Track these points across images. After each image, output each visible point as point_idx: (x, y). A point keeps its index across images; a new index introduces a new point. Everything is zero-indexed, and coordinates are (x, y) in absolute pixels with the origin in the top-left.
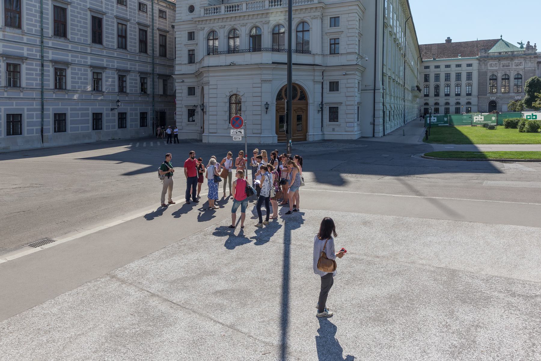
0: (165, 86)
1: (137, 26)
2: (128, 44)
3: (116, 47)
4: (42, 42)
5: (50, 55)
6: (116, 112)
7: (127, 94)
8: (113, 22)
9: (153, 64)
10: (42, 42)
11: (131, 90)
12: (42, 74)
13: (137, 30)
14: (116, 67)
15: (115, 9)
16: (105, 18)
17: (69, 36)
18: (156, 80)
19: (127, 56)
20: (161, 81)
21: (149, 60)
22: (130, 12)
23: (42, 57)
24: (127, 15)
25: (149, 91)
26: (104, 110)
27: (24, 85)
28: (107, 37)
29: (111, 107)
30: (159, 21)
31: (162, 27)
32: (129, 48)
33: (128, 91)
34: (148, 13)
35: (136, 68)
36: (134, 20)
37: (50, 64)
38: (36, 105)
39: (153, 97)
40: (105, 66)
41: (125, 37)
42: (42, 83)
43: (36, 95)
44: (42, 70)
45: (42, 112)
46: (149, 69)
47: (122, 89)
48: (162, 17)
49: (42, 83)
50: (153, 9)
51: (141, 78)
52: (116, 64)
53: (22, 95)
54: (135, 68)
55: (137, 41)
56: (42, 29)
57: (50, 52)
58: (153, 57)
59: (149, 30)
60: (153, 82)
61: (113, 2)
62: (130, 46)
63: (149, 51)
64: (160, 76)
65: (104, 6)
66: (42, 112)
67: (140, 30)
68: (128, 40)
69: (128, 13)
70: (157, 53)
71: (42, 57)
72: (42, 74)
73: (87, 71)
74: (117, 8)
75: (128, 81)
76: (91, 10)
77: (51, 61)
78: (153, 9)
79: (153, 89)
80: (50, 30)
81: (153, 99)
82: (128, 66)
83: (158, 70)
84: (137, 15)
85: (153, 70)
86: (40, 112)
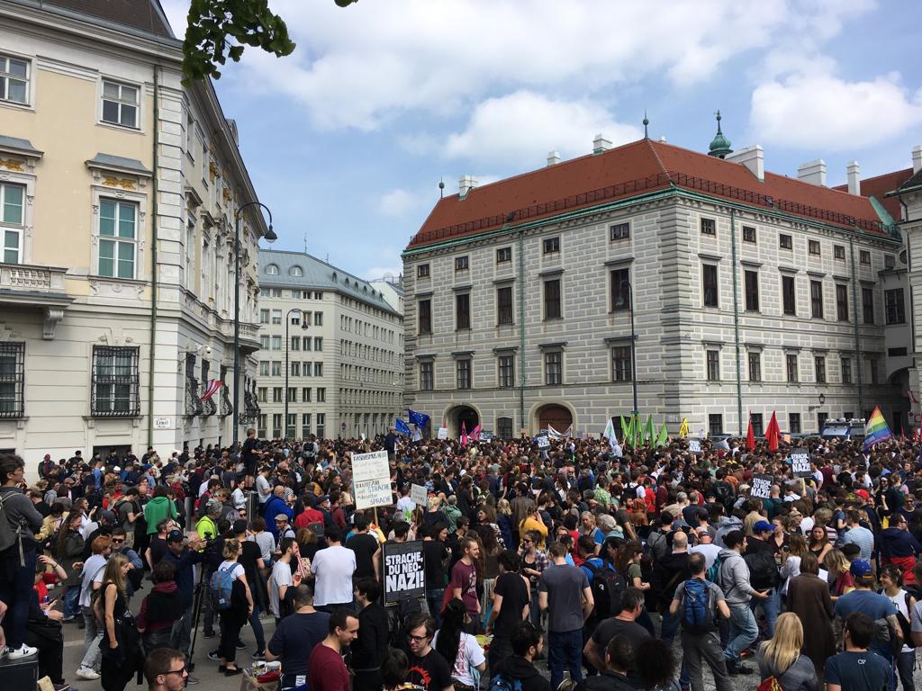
0: (874, 369)
1: (833, 282)
2: (825, 309)
3: (810, 315)
4: (736, 321)
5: (745, 337)
6: (815, 412)
7: (827, 386)
8: (776, 277)
9: (857, 337)
10: (736, 321)
11: (831, 379)
12: (738, 362)
13: (834, 288)
14: (782, 344)
15: (807, 261)
16: (760, 271)
17: (761, 308)
18: (862, 361)
19: (824, 328)
20: (869, 362)
21: (851, 331)
22: (762, 251)
23: (737, 339)
24: (820, 267)
25: (854, 379)
26: (800, 407)
27: (763, 379)
28: (800, 304)
29: (808, 405)
30: (744, 248)
31: (865, 278)
32: (825, 315)
33: (800, 380)
34: (847, 259)
35: (834, 346)
36: (830, 274)
37: (745, 349)
38: (734, 403)
39: (860, 388)
40: (799, 345)
41: (872, 306)
42: (738, 374)
43: (733, 389)
44: (738, 357)
45: (740, 412)
46: (850, 345)
47: (820, 378)
48: (814, 253)
49: (738, 374)
50: (852, 253)
51: (843, 359)
52: (783, 339)
53: (761, 391)
54: (778, 342)
55: (835, 304)
56: (736, 304)
57: (744, 331)
58: (856, 327)
59: (849, 286)
60: (858, 364)
61: (804, 253)
62: (827, 313)
63: (851, 318)
64: (868, 354)
65: (794, 260)
66: (740, 412)
67: (813, 282)
68: (824, 304)
69: (759, 253)
70: (861, 319)
71: (737, 339)
72: (738, 362)
73: (779, 354)
74: (702, 241)
75: (827, 366)
76: (781, 269)
77: (746, 345)
78: (852, 253)
79: (859, 376)
80: (742, 305)
81: (860, 392)
82: (798, 341)
83: (864, 346)
84: (832, 266)
85: (857, 346)
86: (737, 413)
